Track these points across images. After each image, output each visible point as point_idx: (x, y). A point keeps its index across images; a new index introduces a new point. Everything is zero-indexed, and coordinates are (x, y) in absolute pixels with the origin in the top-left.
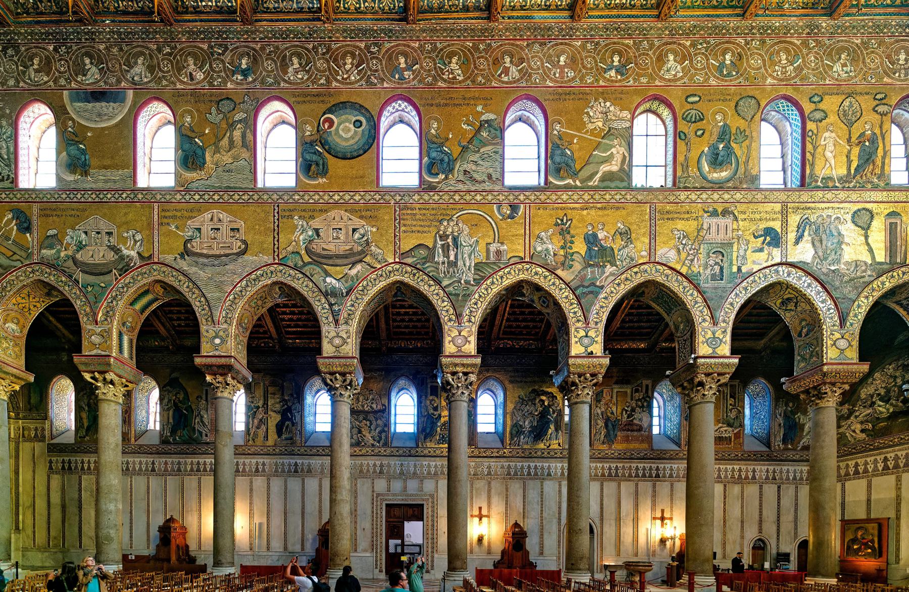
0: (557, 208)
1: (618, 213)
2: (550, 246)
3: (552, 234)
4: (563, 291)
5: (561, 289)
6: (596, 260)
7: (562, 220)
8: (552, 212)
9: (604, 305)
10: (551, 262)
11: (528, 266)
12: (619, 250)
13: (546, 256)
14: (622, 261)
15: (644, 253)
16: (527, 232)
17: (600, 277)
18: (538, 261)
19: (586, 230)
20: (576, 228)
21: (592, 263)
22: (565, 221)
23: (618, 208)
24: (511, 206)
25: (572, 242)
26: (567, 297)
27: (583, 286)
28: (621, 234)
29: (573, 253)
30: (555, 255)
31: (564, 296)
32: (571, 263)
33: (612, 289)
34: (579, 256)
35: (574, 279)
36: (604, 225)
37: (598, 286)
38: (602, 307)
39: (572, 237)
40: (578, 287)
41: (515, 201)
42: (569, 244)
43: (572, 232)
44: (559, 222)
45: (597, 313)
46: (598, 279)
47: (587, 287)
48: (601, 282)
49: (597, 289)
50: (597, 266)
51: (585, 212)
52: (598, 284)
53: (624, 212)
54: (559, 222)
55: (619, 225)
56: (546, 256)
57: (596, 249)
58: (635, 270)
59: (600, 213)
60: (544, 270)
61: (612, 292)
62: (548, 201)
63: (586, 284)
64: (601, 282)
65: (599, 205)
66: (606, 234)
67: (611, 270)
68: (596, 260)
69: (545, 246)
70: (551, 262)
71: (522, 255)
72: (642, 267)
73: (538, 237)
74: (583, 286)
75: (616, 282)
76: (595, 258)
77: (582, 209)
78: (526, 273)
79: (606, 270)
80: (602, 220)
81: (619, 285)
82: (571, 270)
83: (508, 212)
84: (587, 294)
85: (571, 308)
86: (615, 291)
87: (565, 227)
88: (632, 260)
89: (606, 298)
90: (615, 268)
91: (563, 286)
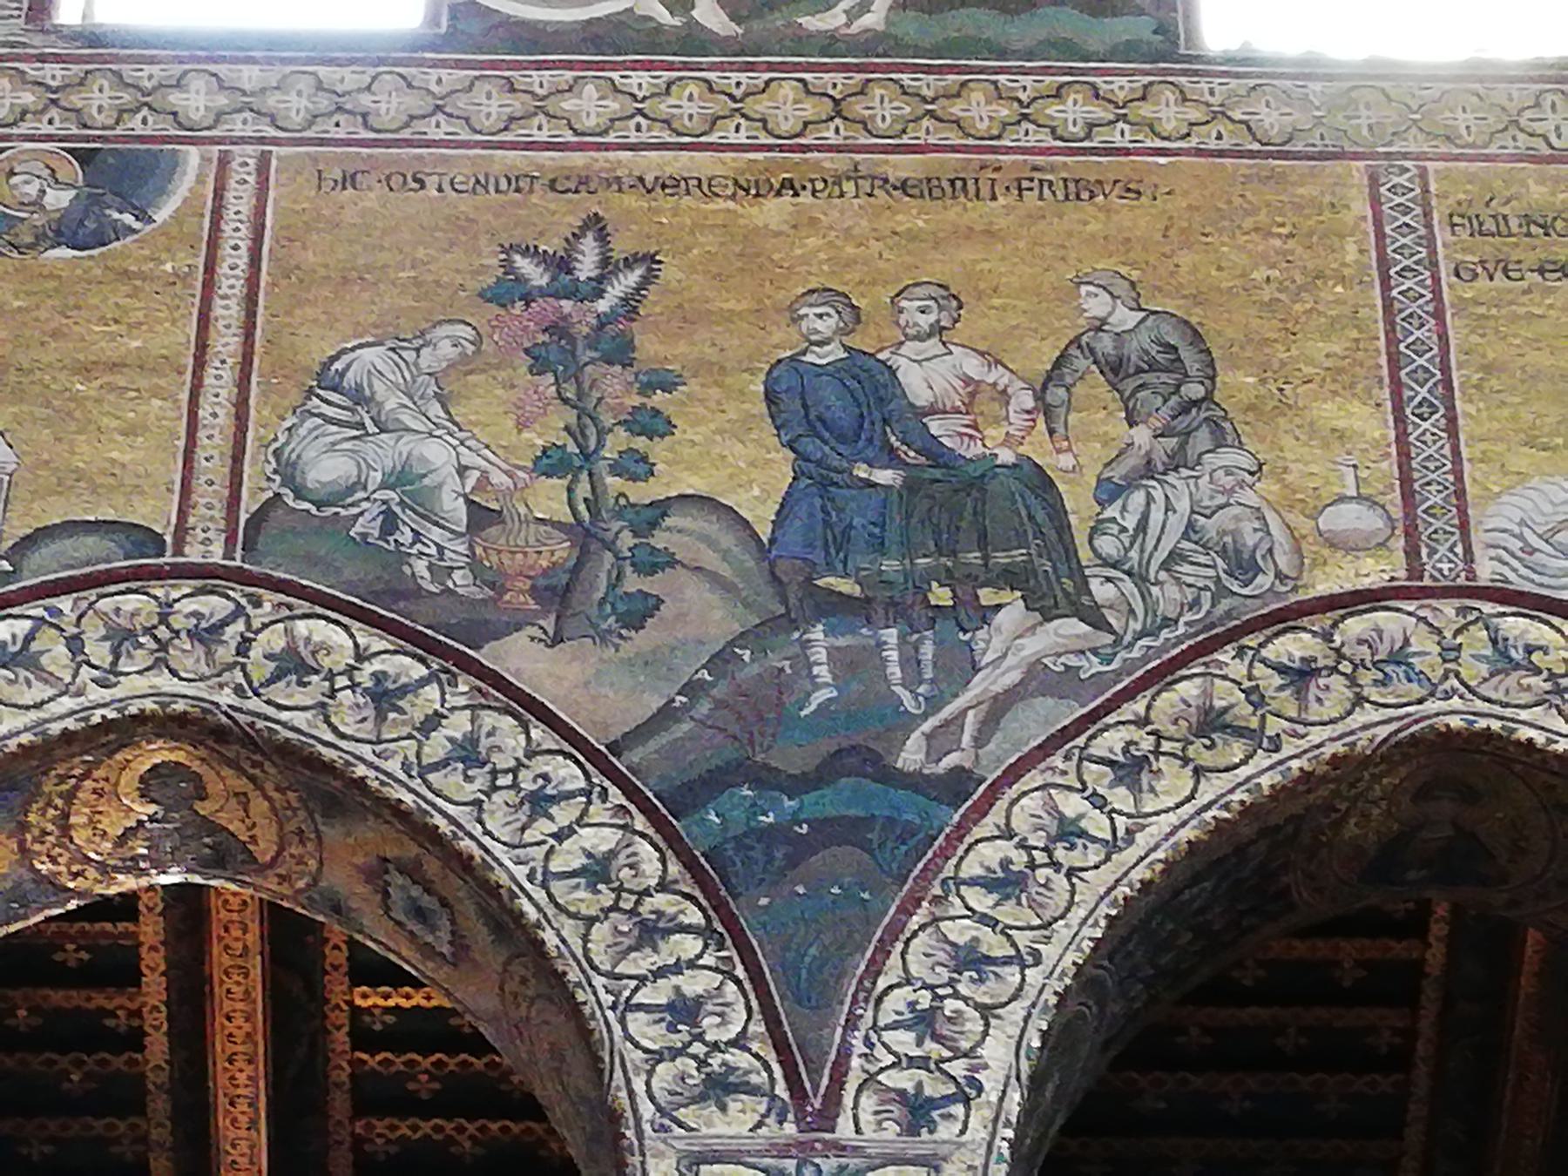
0: (517, 182)
1: (1089, 219)
2: (438, 454)
3: (463, 365)
4: (564, 815)
5: (539, 803)
6: (890, 565)
7: (562, 264)
8: (465, 204)
9: (994, 945)
10: (440, 572)
11: (215, 606)
12: (1109, 492)
13: (390, 523)
14: (1140, 578)
15: (1349, 518)
16: (226, 342)
17: (934, 704)
18: (312, 561)
19: (781, 342)
20: (688, 318)
21: (846, 586)
22: (586, 267)
23: (1080, 190)
24: (84, 158)
25: (653, 425)
26: (597, 871)
27: (766, 779)
28: (1115, 369)
29: (662, 507)
30: (481, 517)
31: (569, 857)
32: (633, 583)
33: (1072, 805)
34: (710, 525)
35: (666, 715)
36: (949, 297)
37: (915, 782)
38: (970, 960)
39: (647, 389)
40: (713, 783)
41: (135, 124)
42: (617, 442)
43: (649, 346)
44: (537, 275)
45: (924, 1022)
46: (909, 723)
47: (799, 785)
48: (939, 742)
49: (910, 807)
50: (897, 611)
51: (774, 211)
52: (911, 755)
53: (1136, 218)
54: (537, 275)
55: (1097, 305)
56: (390, 523)
57: (884, 476)
58: (1292, 647)
59: (913, 216)
60: (374, 641)
61: (1069, 832)
62: (437, 129)
63: (793, 757)
64: (939, 742)
65: (902, 166)
66: (973, 366)
67: (1032, 646)
68: (890, 565)
69: (384, 453)
70: (440, 572)
71: (157, 514)
72: (1356, 626)
73: (327, 378)
74: (766, 779)
75: (1111, 742)
76: (879, 546)
77: (750, 189)
78: (187, 656)
79: (990, 642)
80: (939, 268)
81: (1131, 769)
82: (642, 640)
83: (58, 199)
84: (801, 850)
85: (641, 963)
86: (1097, 825)
87: (582, 316)
88: (1244, 566)
89: (1006, 883)
90: (1074, 627)
91: (567, 774)
